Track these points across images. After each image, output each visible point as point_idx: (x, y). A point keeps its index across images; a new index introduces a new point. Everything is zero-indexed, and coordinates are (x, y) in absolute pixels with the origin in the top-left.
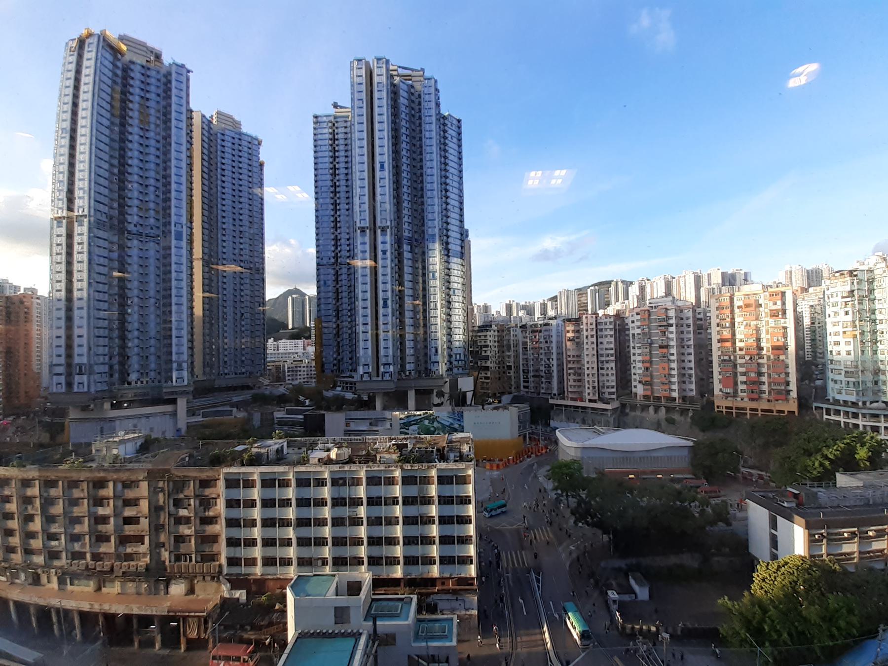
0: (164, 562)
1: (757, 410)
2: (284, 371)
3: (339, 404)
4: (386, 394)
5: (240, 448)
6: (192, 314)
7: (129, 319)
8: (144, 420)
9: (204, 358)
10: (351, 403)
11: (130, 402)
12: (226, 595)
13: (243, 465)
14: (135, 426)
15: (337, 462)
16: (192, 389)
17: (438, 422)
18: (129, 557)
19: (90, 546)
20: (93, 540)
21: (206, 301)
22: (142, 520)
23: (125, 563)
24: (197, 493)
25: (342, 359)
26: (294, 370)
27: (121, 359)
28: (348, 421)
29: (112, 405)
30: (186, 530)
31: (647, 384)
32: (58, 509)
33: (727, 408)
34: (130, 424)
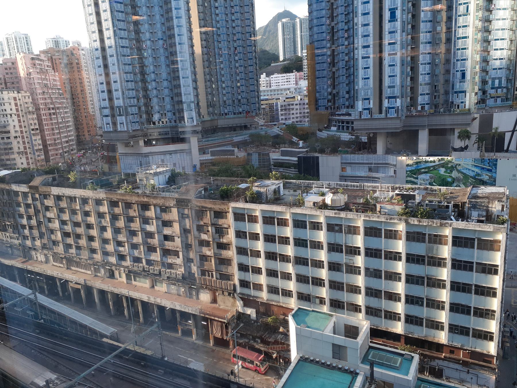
0: (194, 274)
2: (277, 110)
3: (334, 147)
4: (391, 135)
5: (243, 186)
6: (193, 53)
7: (146, 63)
8: (168, 156)
9: (207, 99)
10: (348, 144)
11: (157, 140)
12: (240, 310)
13: (247, 202)
14: (163, 161)
15: (332, 208)
16: (200, 128)
17: (459, 171)
18: (171, 266)
19: (145, 255)
20: (146, 249)
21: (206, 37)
22: (176, 238)
23: (168, 270)
24: (213, 222)
25: (338, 93)
26: (287, 108)
27: (146, 100)
28: (344, 165)
29: (145, 142)
30: (208, 252)
32: (121, 223)
34: (158, 158)
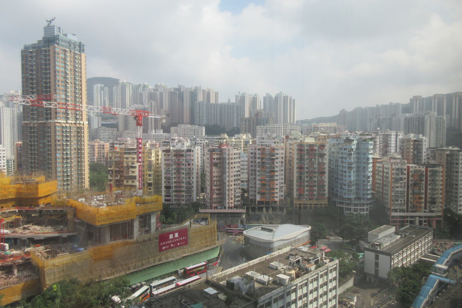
1: (311, 204)
31: (262, 194)
33: (300, 204)
